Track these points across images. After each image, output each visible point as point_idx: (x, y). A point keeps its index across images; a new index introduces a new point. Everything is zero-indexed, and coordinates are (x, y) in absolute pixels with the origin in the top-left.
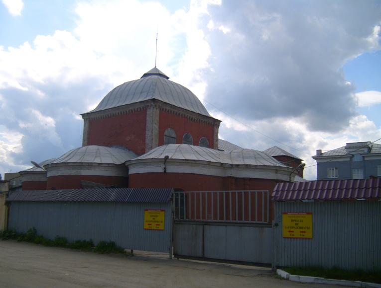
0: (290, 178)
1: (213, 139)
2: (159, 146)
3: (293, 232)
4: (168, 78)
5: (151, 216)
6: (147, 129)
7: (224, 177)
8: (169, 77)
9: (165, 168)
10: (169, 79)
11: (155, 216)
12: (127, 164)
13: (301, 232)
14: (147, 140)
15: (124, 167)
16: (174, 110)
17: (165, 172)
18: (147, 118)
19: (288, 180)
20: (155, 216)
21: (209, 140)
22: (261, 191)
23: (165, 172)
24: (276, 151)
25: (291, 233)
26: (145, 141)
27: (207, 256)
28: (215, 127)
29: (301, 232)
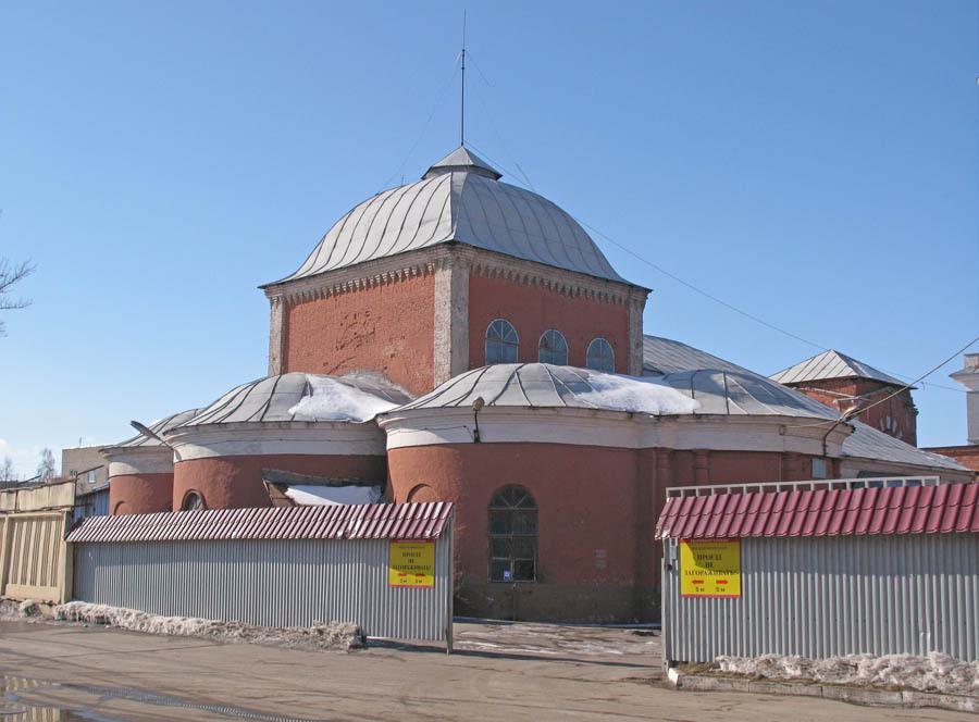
0: (825, 446)
1: (626, 338)
2: (469, 370)
3: (702, 582)
4: (498, 176)
5: (404, 555)
6: (437, 324)
7: (637, 451)
8: (500, 172)
9: (476, 431)
10: (500, 180)
11: (413, 555)
12: (381, 422)
13: (718, 582)
14: (436, 353)
15: (375, 430)
16: (511, 268)
17: (477, 440)
18: (437, 294)
19: (820, 453)
20: (413, 555)
21: (614, 344)
22: (741, 485)
23: (477, 440)
24: (832, 365)
25: (697, 585)
26: (432, 356)
27: (21, 508)
28: (632, 309)
29: (718, 582)
